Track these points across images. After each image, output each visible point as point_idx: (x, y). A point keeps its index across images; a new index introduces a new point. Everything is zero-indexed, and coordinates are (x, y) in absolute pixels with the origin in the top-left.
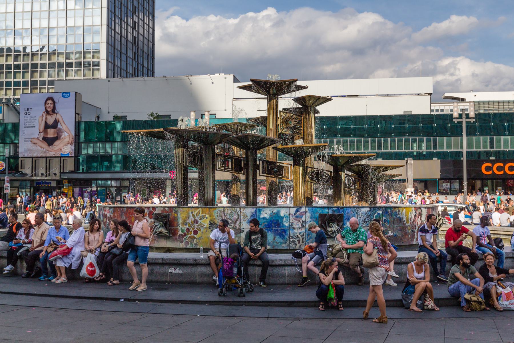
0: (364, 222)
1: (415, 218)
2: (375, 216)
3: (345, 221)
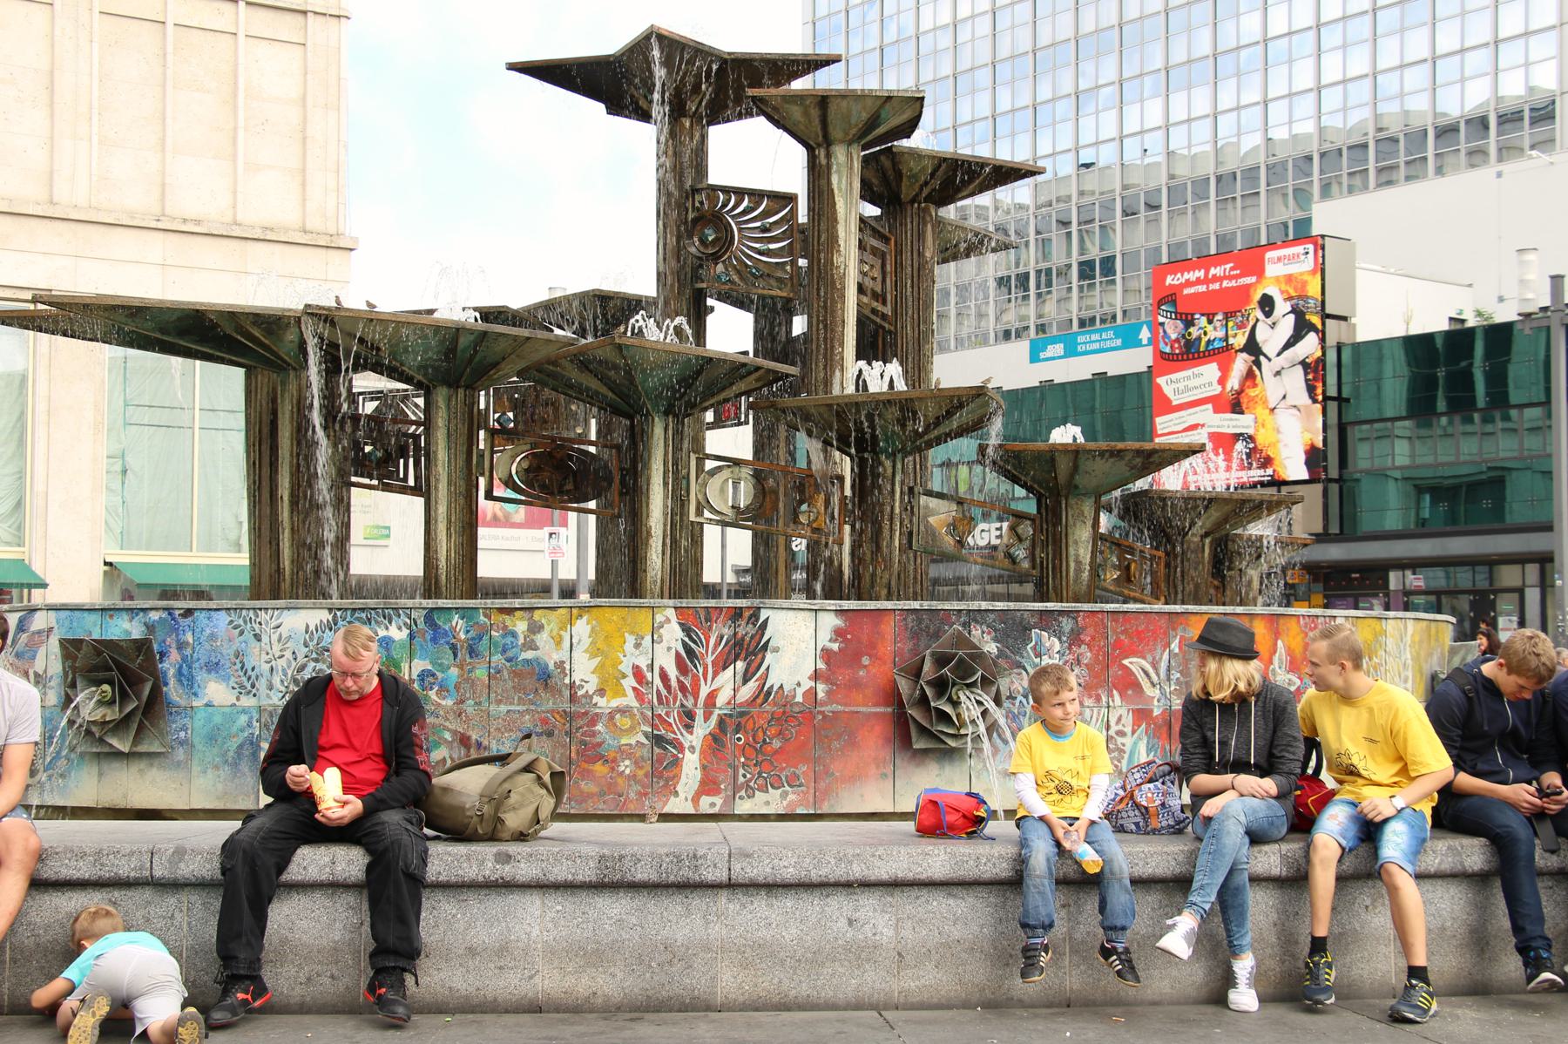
3: (201, 676)
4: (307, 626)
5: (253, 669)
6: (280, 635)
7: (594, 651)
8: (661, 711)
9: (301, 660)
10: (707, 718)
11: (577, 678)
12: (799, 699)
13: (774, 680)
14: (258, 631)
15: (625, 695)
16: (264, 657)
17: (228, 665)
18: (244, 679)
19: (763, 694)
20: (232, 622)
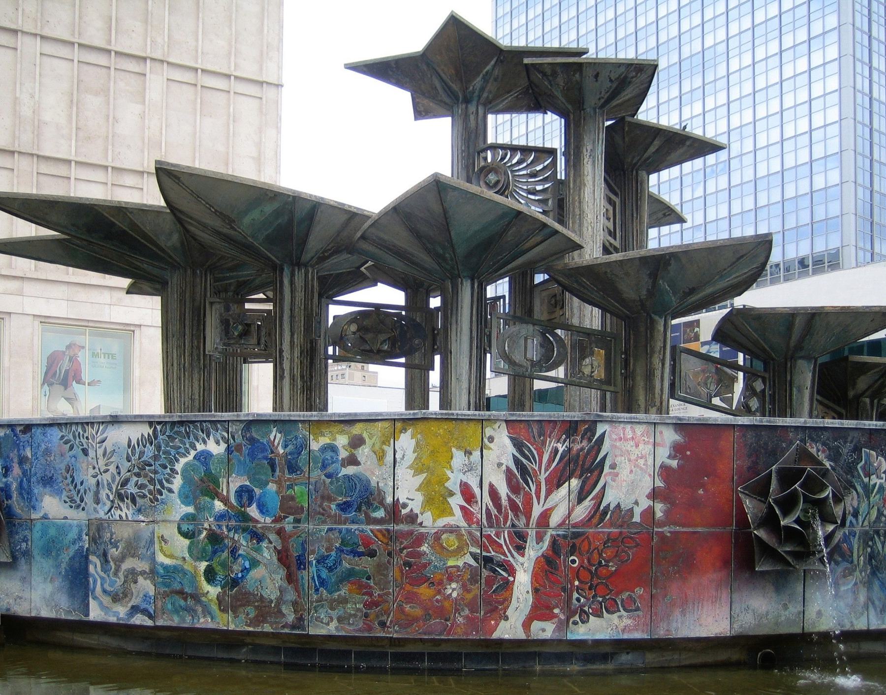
0: (121, 497)
1: (514, 488)
2: (179, 467)
3: (37, 490)
4: (130, 441)
5: (82, 483)
6: (105, 449)
7: (418, 468)
8: (492, 532)
9: (124, 474)
10: (540, 538)
11: (402, 497)
12: (637, 518)
13: (611, 498)
14: (85, 446)
15: (452, 514)
16: (91, 471)
17: (60, 479)
18: (74, 493)
19: (599, 514)
20: (63, 437)
